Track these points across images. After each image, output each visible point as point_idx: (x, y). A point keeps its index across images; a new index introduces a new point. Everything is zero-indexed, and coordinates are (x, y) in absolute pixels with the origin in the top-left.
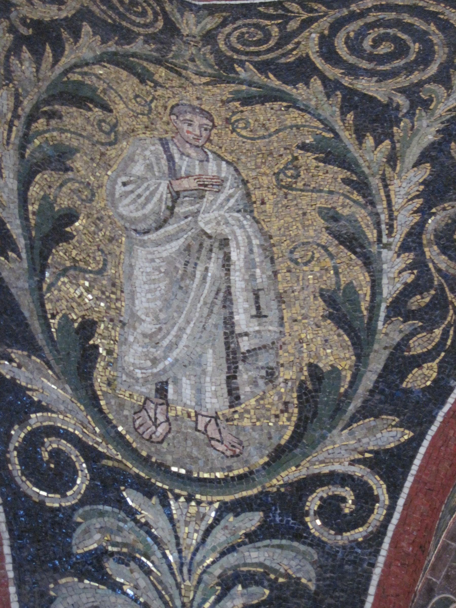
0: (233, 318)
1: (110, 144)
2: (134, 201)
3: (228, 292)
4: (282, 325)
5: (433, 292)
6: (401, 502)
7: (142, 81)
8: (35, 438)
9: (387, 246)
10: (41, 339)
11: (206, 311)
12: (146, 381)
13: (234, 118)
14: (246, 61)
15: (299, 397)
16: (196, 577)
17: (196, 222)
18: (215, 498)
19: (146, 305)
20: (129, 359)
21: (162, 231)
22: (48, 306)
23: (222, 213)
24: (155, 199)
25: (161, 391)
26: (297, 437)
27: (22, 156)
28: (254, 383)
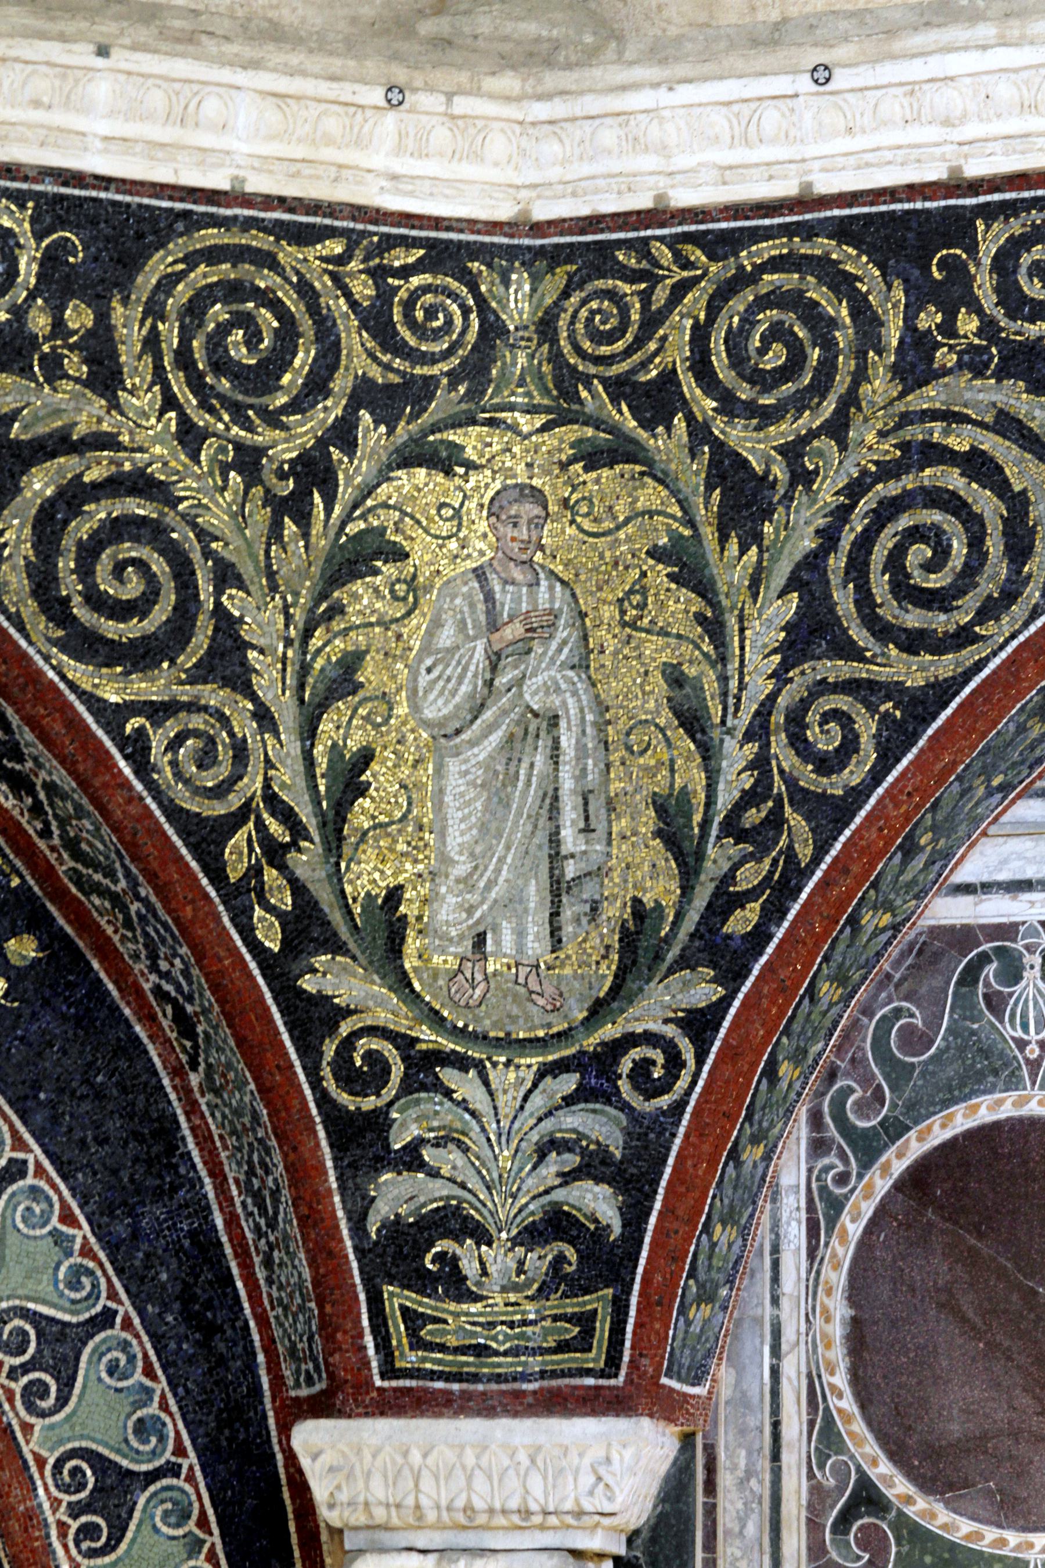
0: (558, 833)
1: (409, 613)
2: (441, 693)
3: (556, 798)
4: (609, 843)
5: (770, 804)
6: (706, 1068)
7: (448, 473)
8: (348, 1044)
9: (730, 732)
10: (344, 932)
11: (529, 828)
12: (462, 937)
13: (574, 497)
14: (595, 376)
15: (621, 940)
16: (514, 1145)
17: (521, 695)
18: (534, 1060)
19: (459, 840)
20: (443, 916)
21: (479, 721)
22: (348, 889)
23: (553, 673)
24: (469, 674)
25: (480, 940)
26: (615, 990)
27: (302, 701)
28: (577, 920)
